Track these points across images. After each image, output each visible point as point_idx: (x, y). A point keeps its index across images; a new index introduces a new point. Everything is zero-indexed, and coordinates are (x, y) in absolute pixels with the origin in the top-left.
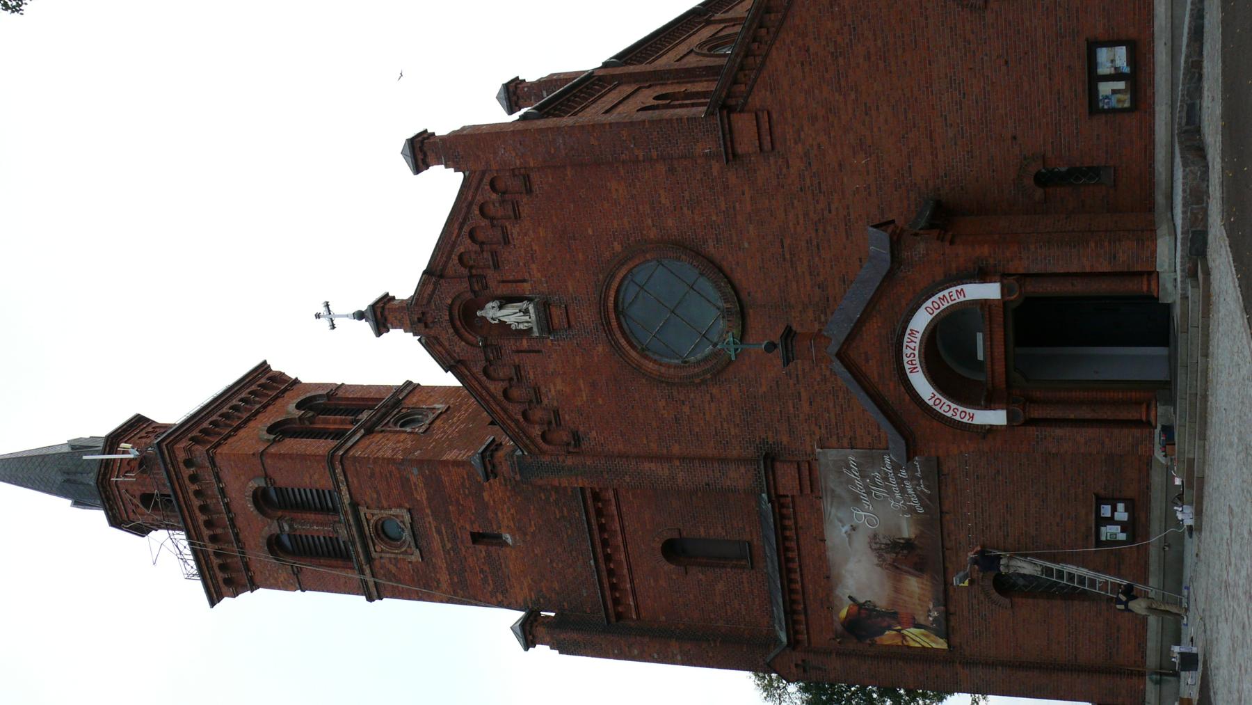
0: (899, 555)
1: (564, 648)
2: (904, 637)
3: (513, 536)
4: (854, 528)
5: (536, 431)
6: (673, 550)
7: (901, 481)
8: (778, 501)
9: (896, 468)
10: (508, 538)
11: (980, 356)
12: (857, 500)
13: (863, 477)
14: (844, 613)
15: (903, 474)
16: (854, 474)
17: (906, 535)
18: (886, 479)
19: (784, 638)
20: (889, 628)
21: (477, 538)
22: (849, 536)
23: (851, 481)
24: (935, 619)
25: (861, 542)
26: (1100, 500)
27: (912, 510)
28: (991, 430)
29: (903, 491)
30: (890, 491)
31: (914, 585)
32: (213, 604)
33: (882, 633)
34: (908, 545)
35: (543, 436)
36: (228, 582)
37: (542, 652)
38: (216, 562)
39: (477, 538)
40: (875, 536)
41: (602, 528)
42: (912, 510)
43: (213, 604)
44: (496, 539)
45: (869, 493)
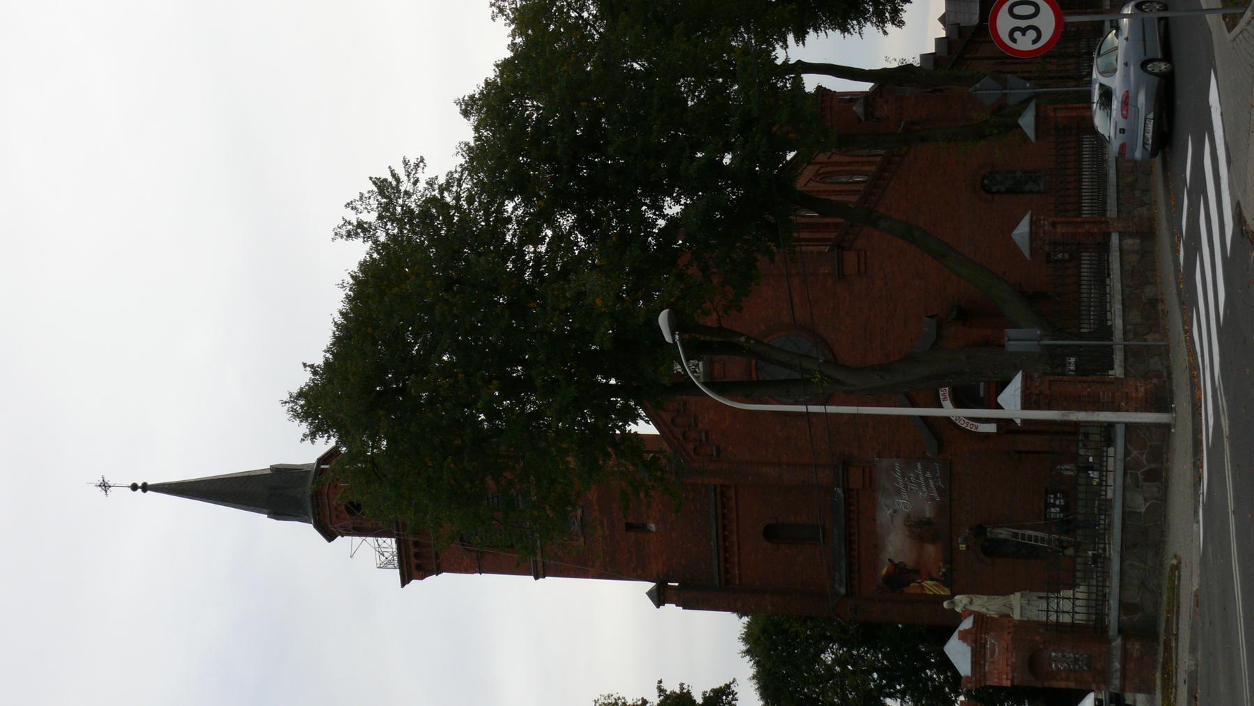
0: (920, 530)
1: (687, 605)
2: (922, 587)
3: (657, 525)
4: (895, 511)
5: (691, 446)
6: (770, 533)
7: (926, 479)
8: (847, 491)
9: (924, 472)
10: (653, 527)
11: (982, 394)
12: (898, 492)
13: (903, 476)
14: (884, 571)
15: (928, 475)
16: (898, 475)
17: (928, 515)
18: (917, 478)
19: (843, 591)
20: (914, 581)
21: (629, 527)
22: (892, 516)
23: (896, 480)
24: (944, 574)
25: (899, 521)
26: (1047, 492)
27: (932, 499)
28: (987, 435)
29: (928, 486)
30: (920, 487)
31: (931, 550)
32: (403, 585)
33: (908, 585)
34: (929, 522)
35: (695, 450)
36: (419, 567)
37: (670, 608)
38: (413, 550)
39: (629, 527)
40: (908, 516)
41: (724, 516)
42: (932, 499)
43: (403, 585)
44: (643, 528)
45: (906, 487)
